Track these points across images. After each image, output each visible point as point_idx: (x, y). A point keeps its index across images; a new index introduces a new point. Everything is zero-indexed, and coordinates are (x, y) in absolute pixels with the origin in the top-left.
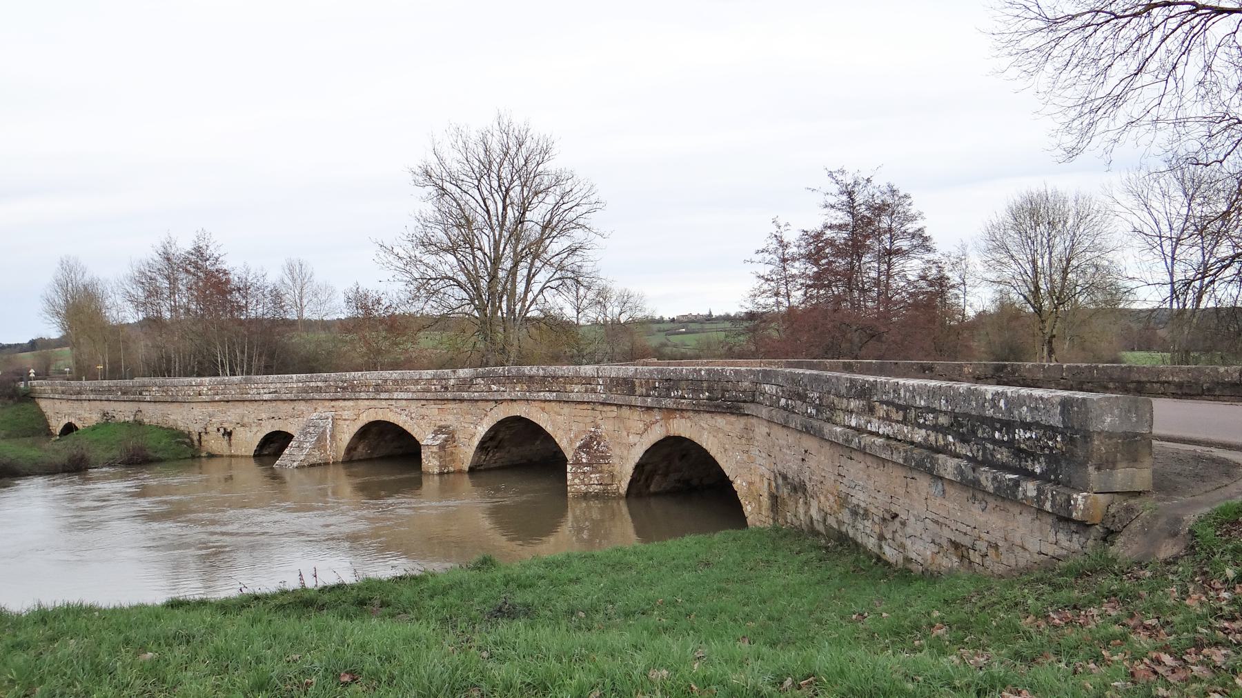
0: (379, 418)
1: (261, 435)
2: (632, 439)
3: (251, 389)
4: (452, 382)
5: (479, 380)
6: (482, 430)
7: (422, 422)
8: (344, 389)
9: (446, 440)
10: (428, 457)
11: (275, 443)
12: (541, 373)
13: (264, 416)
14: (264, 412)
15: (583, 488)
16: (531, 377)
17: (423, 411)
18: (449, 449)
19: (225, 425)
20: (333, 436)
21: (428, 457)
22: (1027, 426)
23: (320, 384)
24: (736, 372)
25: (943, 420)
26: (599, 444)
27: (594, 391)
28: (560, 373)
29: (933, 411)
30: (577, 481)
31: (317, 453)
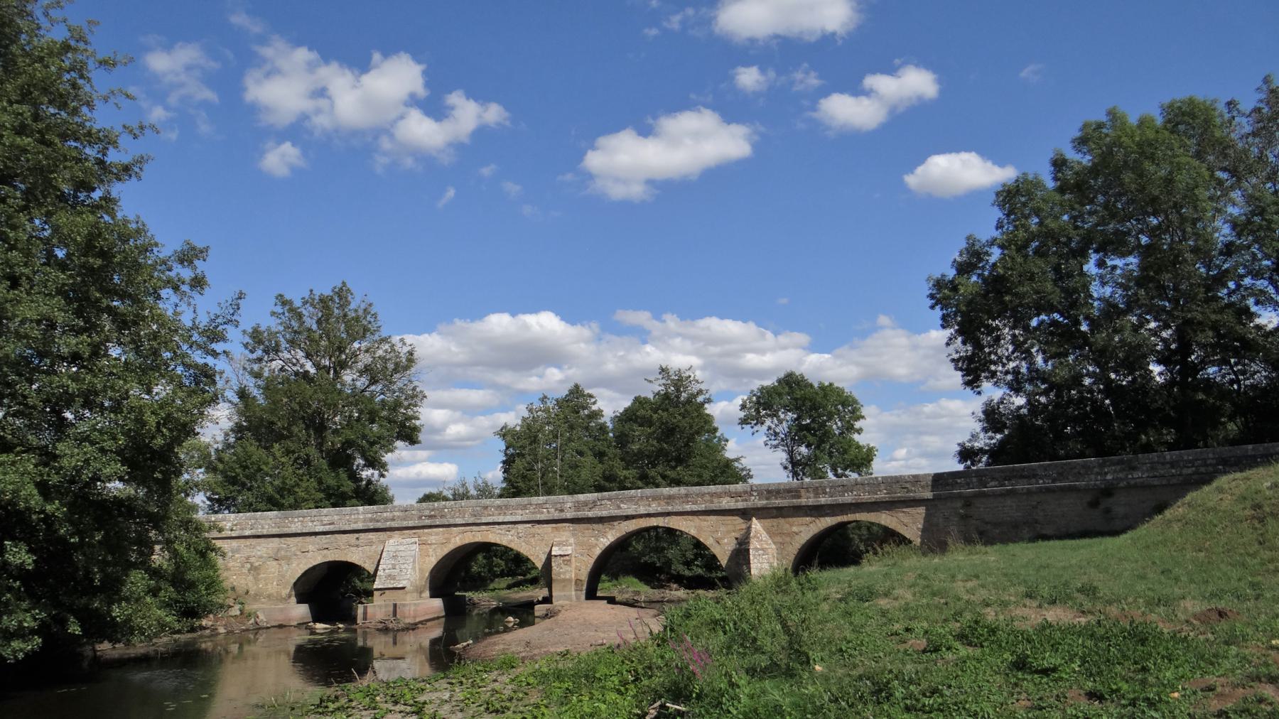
2: (795, 529)
3: (291, 522)
4: (569, 505)
8: (431, 517)
13: (311, 547)
14: (311, 543)
17: (533, 530)
19: (252, 560)
23: (397, 514)
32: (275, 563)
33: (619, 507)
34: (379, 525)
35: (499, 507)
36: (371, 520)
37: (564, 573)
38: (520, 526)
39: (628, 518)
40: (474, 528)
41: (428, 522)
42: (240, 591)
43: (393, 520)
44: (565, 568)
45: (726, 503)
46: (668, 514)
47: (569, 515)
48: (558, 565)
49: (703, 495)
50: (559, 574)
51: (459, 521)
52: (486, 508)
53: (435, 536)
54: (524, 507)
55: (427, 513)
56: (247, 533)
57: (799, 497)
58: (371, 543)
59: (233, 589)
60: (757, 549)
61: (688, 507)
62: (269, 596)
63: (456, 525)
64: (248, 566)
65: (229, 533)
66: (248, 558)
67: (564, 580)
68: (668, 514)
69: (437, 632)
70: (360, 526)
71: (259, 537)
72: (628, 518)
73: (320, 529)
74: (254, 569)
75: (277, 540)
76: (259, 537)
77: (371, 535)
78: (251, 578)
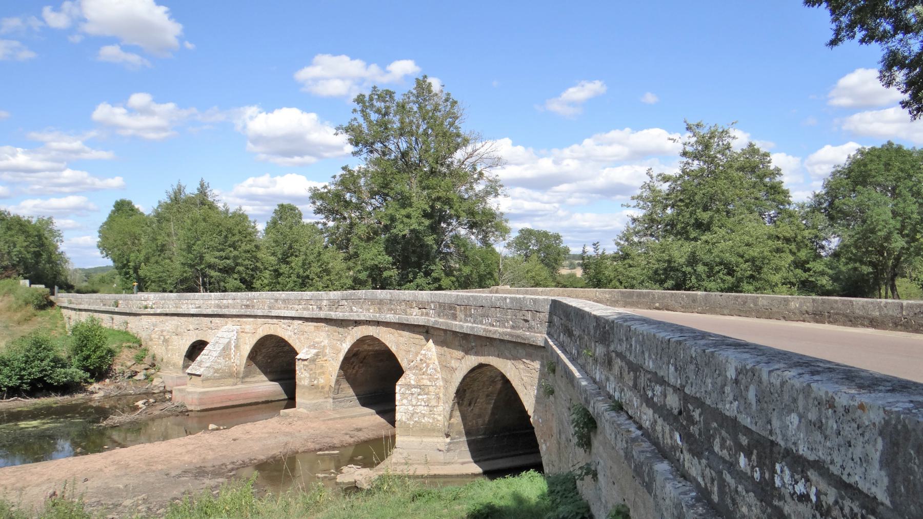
0: (271, 332)
1: (189, 343)
4: (325, 303)
5: (344, 302)
6: (346, 347)
8: (247, 306)
9: (317, 355)
10: (300, 369)
11: (197, 348)
12: (389, 296)
13: (191, 327)
15: (411, 408)
16: (381, 300)
18: (319, 362)
19: (165, 333)
20: (237, 347)
21: (300, 369)
22: (799, 465)
23: (230, 301)
24: (535, 301)
25: (673, 401)
26: (428, 366)
27: (427, 314)
28: (403, 297)
29: (663, 382)
30: (405, 401)
31: (221, 360)
32: (176, 337)
33: (352, 310)
34: (220, 312)
35: (284, 301)
36: (219, 306)
38: (296, 322)
39: (357, 323)
40: (270, 321)
41: (243, 312)
42: (158, 358)
43: (228, 307)
45: (416, 317)
46: (378, 323)
47: (322, 315)
49: (400, 302)
50: (301, 379)
51: (259, 313)
52: (276, 300)
53: (249, 324)
54: (299, 301)
55: (245, 302)
56: (158, 311)
57: (454, 317)
58: (217, 328)
59: (154, 357)
60: (409, 386)
61: (390, 317)
62: (174, 365)
63: (255, 317)
65: (149, 311)
66: (162, 331)
68: (378, 323)
70: (209, 312)
71: (167, 315)
72: (357, 323)
73: (193, 311)
74: (166, 341)
75: (176, 318)
76: (167, 315)
77: (217, 320)
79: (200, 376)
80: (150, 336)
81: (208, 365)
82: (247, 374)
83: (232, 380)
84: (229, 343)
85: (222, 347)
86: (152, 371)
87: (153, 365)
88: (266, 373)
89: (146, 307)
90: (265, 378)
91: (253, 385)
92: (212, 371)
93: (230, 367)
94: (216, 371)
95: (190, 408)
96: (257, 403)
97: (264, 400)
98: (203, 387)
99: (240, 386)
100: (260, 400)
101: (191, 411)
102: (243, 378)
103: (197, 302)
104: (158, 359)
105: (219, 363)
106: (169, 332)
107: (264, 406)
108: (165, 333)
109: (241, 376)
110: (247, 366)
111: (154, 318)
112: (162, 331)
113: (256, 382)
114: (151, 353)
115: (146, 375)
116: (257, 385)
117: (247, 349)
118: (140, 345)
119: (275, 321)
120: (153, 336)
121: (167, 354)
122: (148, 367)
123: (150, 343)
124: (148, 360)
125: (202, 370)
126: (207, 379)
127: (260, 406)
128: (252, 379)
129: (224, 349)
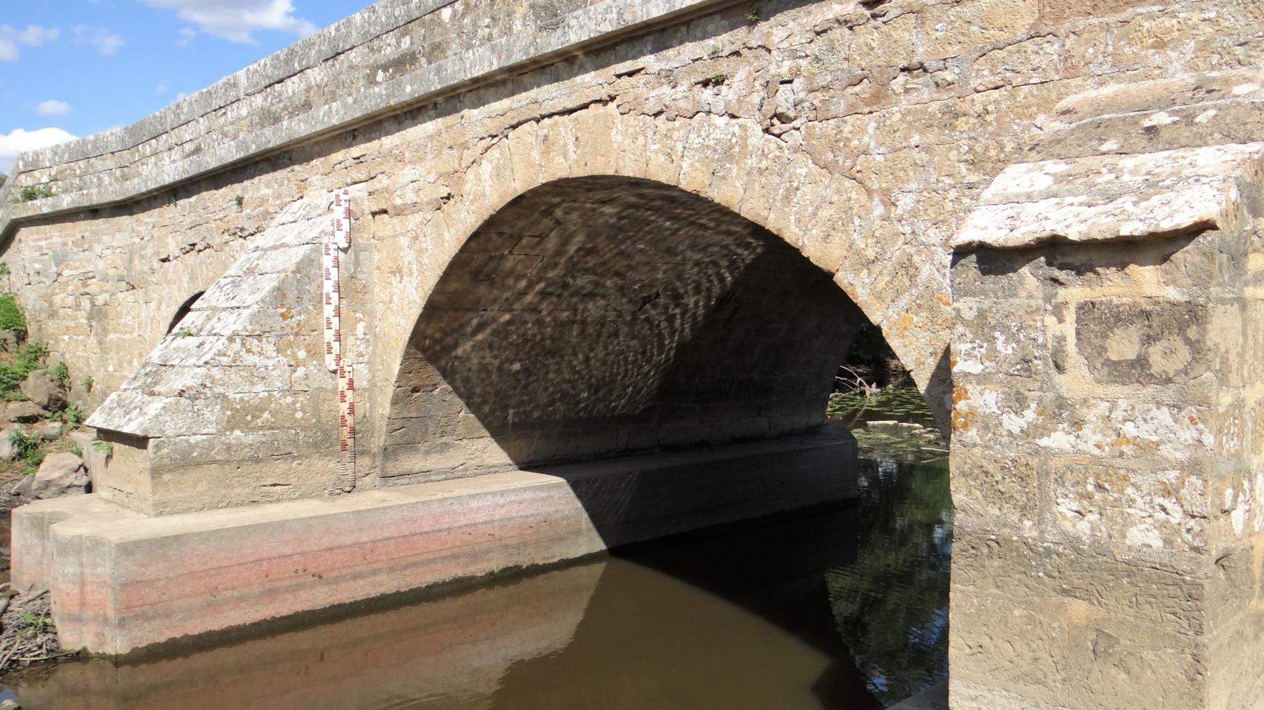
0: (567, 163)
7: (866, 131)
8: (402, 63)
31: (267, 357)
32: (129, 297)
37: (1102, 479)
40: (551, 94)
42: (77, 379)
44: (1113, 417)
48: (1027, 372)
50: (1030, 480)
53: (411, 161)
55: (390, 48)
56: (66, 202)
59: (63, 376)
64: (86, 303)
66: (86, 279)
67: (1093, 569)
69: (549, 630)
71: (94, 212)
75: (124, 221)
76: (94, 212)
78: (92, 341)
79: (139, 442)
80: (48, 298)
81: (188, 379)
82: (409, 433)
83: (330, 468)
84: (306, 268)
85: (268, 284)
86: (52, 427)
87: (57, 405)
88: (499, 432)
89: (30, 195)
90: (495, 454)
91: (436, 492)
92: (213, 414)
93: (317, 397)
94: (240, 417)
95: (70, 639)
96: (462, 587)
97: (496, 564)
98: (161, 509)
99: (372, 498)
100: (479, 569)
101: (80, 657)
102: (388, 453)
103: (186, 133)
104: (78, 383)
105: (255, 376)
106: (105, 279)
107: (498, 593)
108: (94, 286)
109: (379, 441)
110: (409, 390)
111: (55, 234)
112: (86, 279)
113: (452, 474)
114: (53, 362)
115: (20, 441)
116: (459, 489)
117: (402, 301)
118: (21, 336)
119: (590, 82)
120: (57, 300)
121: (103, 362)
122: (30, 409)
123: (51, 327)
124: (36, 388)
125: (155, 407)
126: (185, 462)
127: (479, 597)
128: (435, 462)
129: (279, 294)
